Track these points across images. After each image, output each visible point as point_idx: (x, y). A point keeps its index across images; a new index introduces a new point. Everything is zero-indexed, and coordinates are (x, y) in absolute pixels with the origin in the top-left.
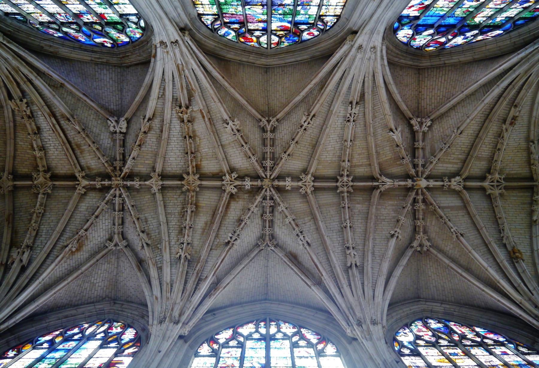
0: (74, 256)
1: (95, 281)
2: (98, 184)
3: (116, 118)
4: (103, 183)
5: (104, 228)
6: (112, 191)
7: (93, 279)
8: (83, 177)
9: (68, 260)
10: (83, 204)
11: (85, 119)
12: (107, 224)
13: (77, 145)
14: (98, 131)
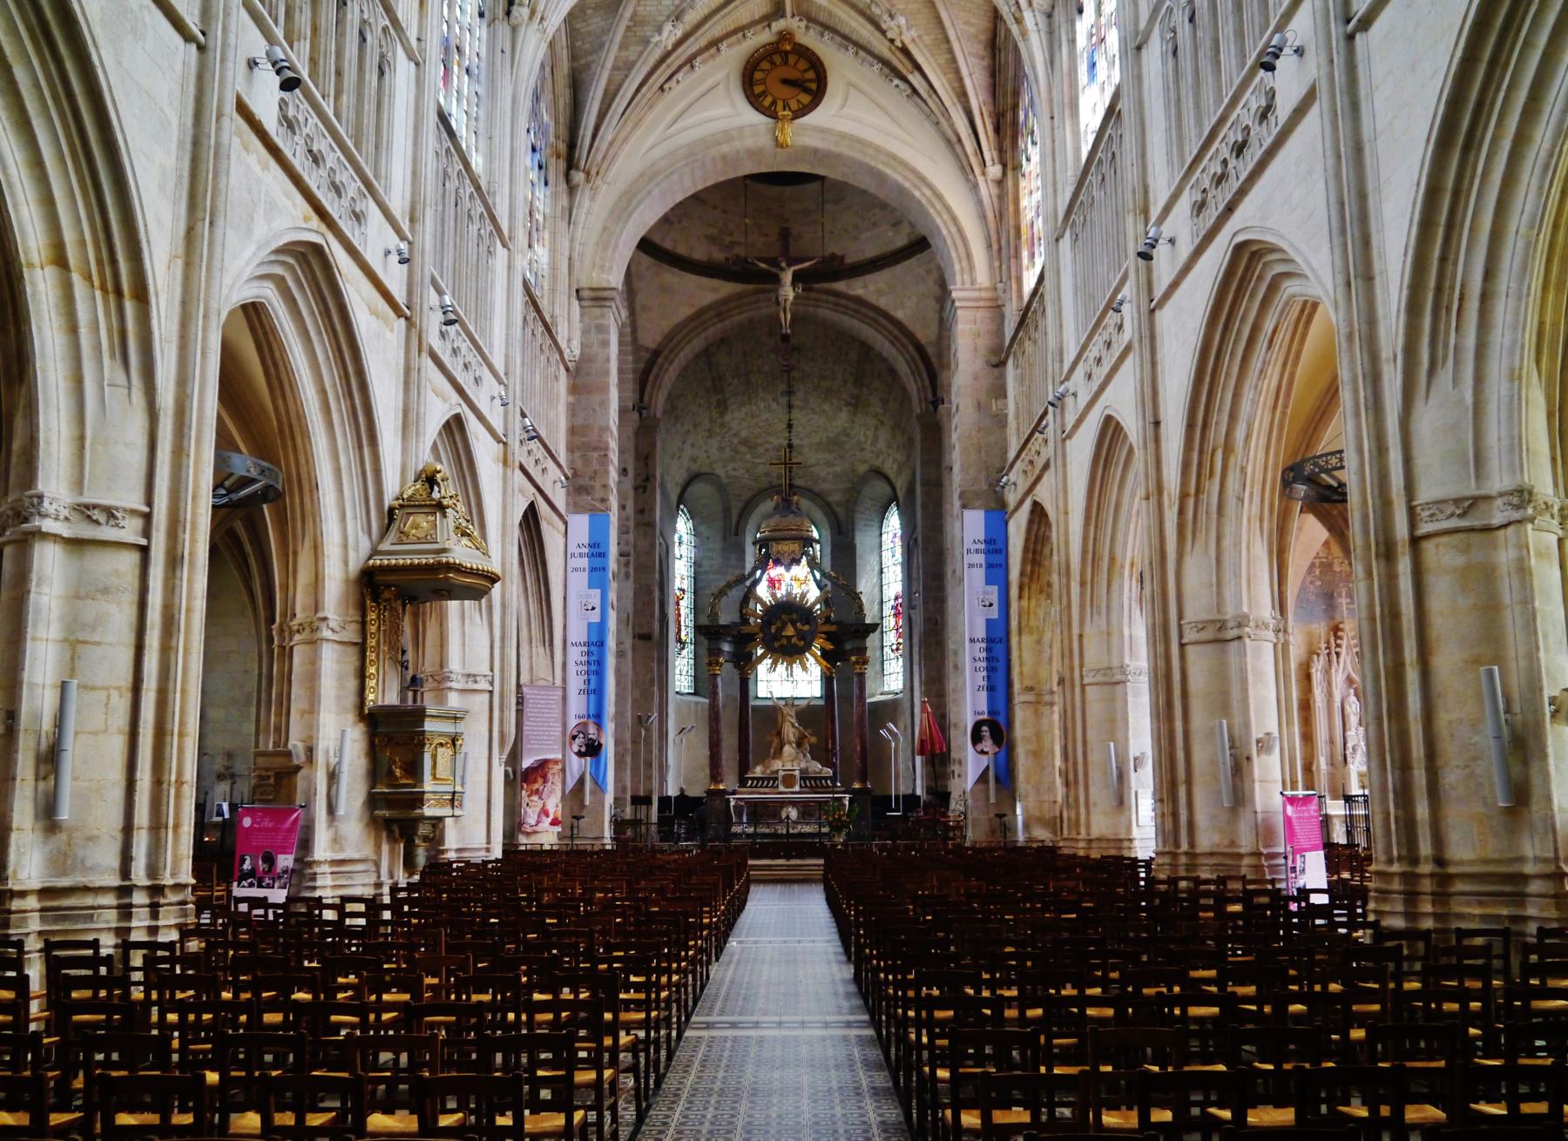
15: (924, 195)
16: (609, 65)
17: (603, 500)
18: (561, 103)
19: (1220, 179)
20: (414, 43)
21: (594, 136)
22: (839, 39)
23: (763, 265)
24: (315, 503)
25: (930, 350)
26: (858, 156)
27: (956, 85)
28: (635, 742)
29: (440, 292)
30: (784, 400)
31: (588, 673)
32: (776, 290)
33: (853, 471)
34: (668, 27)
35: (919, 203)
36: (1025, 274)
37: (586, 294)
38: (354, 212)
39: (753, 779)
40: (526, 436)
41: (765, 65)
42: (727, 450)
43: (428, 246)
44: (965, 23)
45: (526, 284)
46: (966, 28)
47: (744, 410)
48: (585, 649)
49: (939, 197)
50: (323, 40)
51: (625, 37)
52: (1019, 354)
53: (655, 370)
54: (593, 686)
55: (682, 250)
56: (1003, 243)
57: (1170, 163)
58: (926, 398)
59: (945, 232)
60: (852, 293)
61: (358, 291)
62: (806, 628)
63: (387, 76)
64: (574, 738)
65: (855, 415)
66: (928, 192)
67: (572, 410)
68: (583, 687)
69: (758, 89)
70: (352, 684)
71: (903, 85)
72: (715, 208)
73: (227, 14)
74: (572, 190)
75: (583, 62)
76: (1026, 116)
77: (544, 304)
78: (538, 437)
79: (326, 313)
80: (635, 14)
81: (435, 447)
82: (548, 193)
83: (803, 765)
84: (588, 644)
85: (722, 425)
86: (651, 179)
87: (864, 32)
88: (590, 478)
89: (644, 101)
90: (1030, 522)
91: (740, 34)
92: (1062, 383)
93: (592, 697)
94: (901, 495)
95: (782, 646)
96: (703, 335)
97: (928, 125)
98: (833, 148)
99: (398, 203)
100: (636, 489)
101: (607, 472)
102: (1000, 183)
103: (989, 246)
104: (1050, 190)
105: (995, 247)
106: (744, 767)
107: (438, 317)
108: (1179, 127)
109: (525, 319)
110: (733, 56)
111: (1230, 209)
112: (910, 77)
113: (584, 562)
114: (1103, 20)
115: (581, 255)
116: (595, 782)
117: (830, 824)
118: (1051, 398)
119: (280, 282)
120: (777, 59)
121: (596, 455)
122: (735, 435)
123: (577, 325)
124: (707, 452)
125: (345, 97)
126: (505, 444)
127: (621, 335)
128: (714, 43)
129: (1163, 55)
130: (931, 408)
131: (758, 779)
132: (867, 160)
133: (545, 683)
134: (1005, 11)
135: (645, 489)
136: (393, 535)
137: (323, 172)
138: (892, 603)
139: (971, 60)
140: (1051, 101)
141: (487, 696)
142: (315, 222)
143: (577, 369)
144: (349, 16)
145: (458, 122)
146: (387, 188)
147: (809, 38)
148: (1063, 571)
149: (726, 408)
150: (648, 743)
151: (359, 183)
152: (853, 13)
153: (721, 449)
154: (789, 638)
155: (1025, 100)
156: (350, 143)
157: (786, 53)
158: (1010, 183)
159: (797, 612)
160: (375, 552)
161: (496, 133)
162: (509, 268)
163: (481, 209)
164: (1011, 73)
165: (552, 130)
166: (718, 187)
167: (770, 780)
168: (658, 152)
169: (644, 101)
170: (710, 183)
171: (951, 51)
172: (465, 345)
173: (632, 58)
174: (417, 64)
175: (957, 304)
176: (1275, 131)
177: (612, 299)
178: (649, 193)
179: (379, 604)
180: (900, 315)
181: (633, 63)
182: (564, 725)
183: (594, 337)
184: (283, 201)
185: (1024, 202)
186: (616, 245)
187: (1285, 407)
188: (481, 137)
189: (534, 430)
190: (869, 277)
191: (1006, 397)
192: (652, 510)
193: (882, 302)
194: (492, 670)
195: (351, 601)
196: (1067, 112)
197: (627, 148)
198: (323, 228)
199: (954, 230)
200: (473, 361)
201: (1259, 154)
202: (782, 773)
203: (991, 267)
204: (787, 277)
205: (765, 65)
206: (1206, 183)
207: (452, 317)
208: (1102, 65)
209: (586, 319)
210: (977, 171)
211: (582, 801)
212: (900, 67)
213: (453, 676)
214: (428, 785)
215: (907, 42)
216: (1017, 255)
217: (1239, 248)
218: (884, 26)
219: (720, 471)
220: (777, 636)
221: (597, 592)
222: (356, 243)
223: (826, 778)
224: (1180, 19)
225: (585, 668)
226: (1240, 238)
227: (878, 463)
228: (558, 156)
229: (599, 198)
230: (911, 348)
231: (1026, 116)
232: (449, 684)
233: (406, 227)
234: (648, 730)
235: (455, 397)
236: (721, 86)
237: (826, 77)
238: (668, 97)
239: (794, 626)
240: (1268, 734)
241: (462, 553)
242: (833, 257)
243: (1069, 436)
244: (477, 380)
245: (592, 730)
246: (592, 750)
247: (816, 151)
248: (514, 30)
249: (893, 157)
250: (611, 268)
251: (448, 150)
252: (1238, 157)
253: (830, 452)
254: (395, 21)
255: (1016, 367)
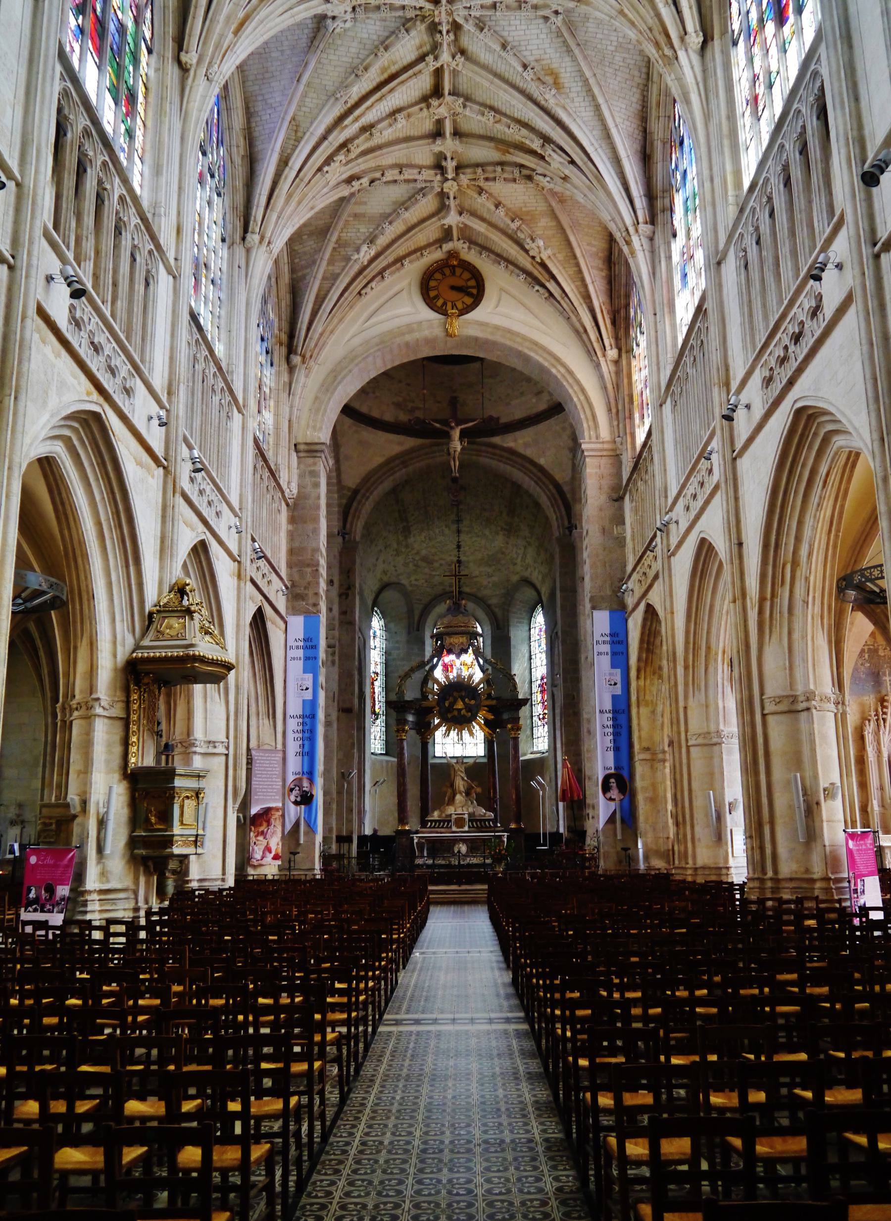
0: (566, 85)
1: (615, 44)
2: (447, 39)
3: (329, 21)
4: (444, 33)
5: (524, 27)
6: (460, 21)
7: (609, 48)
8: (436, 58)
9: (571, 95)
10: (482, 56)
11: (338, 69)
12: (518, 22)
13: (383, 73)
14: (355, 44)
15: (559, 371)
16: (320, 276)
17: (315, 605)
18: (283, 304)
19: (783, 361)
20: (172, 261)
21: (308, 329)
22: (492, 256)
23: (438, 425)
24: (92, 609)
25: (566, 489)
26: (508, 343)
27: (582, 290)
28: (340, 793)
29: (190, 448)
30: (454, 527)
31: (302, 739)
32: (448, 444)
33: (508, 581)
34: (364, 248)
35: (556, 377)
36: (637, 430)
37: (302, 447)
38: (125, 388)
39: (431, 821)
40: (255, 556)
41: (438, 276)
42: (411, 565)
43: (181, 413)
44: (589, 244)
45: (256, 441)
46: (588, 248)
47: (424, 534)
48: (301, 720)
49: (571, 373)
50: (103, 260)
51: (331, 255)
52: (634, 491)
53: (355, 504)
54: (306, 749)
55: (375, 414)
56: (620, 408)
57: (745, 348)
58: (563, 525)
59: (575, 399)
60: (505, 445)
61: (127, 448)
62: (473, 702)
63: (151, 287)
64: (291, 790)
65: (509, 537)
66: (562, 370)
67: (291, 536)
68: (299, 750)
69: (432, 294)
70: (118, 750)
71: (542, 290)
72: (400, 381)
73: (31, 242)
74: (291, 369)
75: (300, 274)
76: (636, 313)
77: (270, 455)
78: (265, 557)
79: (102, 464)
80: (339, 239)
81: (185, 565)
82: (273, 371)
83: (471, 810)
84: (303, 716)
85: (407, 546)
86: (352, 360)
87: (512, 251)
88: (305, 588)
89: (346, 304)
90: (645, 620)
91: (419, 254)
92: (667, 513)
93: (306, 758)
94: (544, 599)
95: (454, 717)
96: (392, 478)
97: (561, 319)
98: (490, 337)
99: (159, 382)
100: (340, 595)
101: (318, 583)
102: (617, 362)
103: (610, 410)
104: (655, 368)
105: (614, 411)
106: (424, 812)
107: (189, 466)
108: (751, 322)
109: (255, 467)
110: (414, 268)
111: (791, 383)
112: (548, 284)
113: (300, 653)
114: (692, 243)
115: (298, 418)
116: (308, 824)
117: (493, 857)
118: (658, 525)
119: (67, 442)
120: (447, 271)
121: (309, 570)
122: (417, 553)
123: (295, 472)
125: (119, 302)
126: (239, 562)
127: (329, 478)
128: (400, 260)
129: (738, 269)
130: (567, 532)
131: (436, 821)
132: (516, 346)
133: (269, 748)
134: (618, 236)
135: (347, 595)
136: (151, 634)
137: (102, 359)
138: (539, 682)
139: (594, 272)
140: (654, 302)
141: (224, 758)
142: (95, 396)
143: (295, 504)
144: (123, 242)
145: (205, 320)
146: (151, 370)
147: (471, 256)
148: (671, 658)
149: (410, 533)
150: (350, 793)
151: (129, 366)
152: (503, 237)
153: (406, 565)
154: (459, 710)
155: (634, 300)
156: (122, 336)
157: (454, 267)
158: (624, 362)
160: (137, 647)
161: (234, 327)
162: (243, 428)
163: (222, 384)
164: (623, 281)
165: (276, 325)
166: (402, 366)
167: (445, 822)
168: (357, 341)
169: (346, 304)
170: (397, 363)
171: (578, 265)
172: (209, 488)
173: (338, 271)
174: (174, 277)
175: (586, 453)
176: (823, 325)
177: (322, 451)
178: (350, 371)
179: (140, 688)
180: (542, 461)
181: (339, 275)
182: (284, 780)
183: (308, 480)
184: (71, 380)
185: (635, 377)
186: (325, 410)
187: (838, 531)
188: (222, 331)
189: (262, 551)
190: (518, 434)
191: (624, 524)
192: (353, 612)
193: (529, 452)
194: (228, 738)
195: (118, 685)
196: (666, 310)
197: (333, 338)
198: (101, 400)
199: (582, 398)
200: (215, 499)
201: (811, 342)
202: (454, 817)
203: (611, 425)
204: (456, 434)
205: (438, 276)
206: (773, 363)
207: (199, 466)
208: (691, 276)
209: (302, 466)
210: (599, 353)
211: (298, 840)
212: (540, 277)
213: (197, 743)
214: (177, 830)
215: (544, 258)
216: (631, 417)
217: (799, 412)
218: (527, 247)
219: (404, 581)
220: (450, 709)
221: (310, 676)
222: (126, 411)
223: (489, 820)
224: (749, 241)
225: (300, 735)
226: (799, 405)
227: (526, 574)
228: (281, 344)
229: (312, 376)
230: (551, 487)
231: (636, 313)
232: (194, 749)
233: (164, 399)
234: (350, 784)
235: (201, 527)
236: (404, 293)
237: (484, 285)
238: (365, 300)
239: (463, 701)
240: (832, 784)
241: (205, 647)
242: (491, 418)
243: (673, 554)
244: (218, 514)
245: (306, 784)
246: (306, 799)
247: (476, 339)
248: (248, 251)
249: (536, 344)
250: (321, 428)
251: (197, 341)
252: (795, 344)
253: (490, 566)
254: (158, 246)
255: (632, 501)
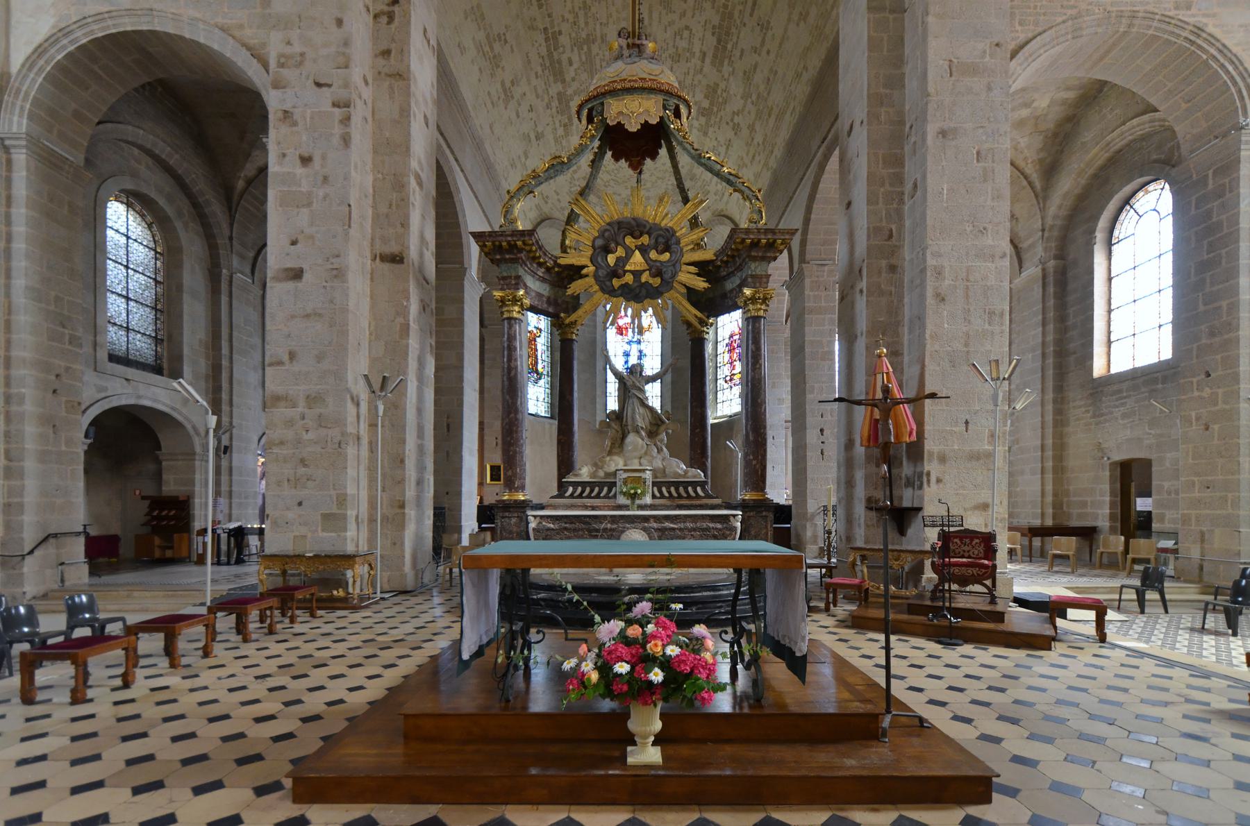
39: (575, 484)
65: (706, 134)
83: (658, 463)
95: (625, 286)
124: (558, 194)
131: (584, 484)
150: (397, 426)
154: (637, 274)
159: (649, 234)
223: (694, 484)
227: (721, 206)
239: (644, 250)
